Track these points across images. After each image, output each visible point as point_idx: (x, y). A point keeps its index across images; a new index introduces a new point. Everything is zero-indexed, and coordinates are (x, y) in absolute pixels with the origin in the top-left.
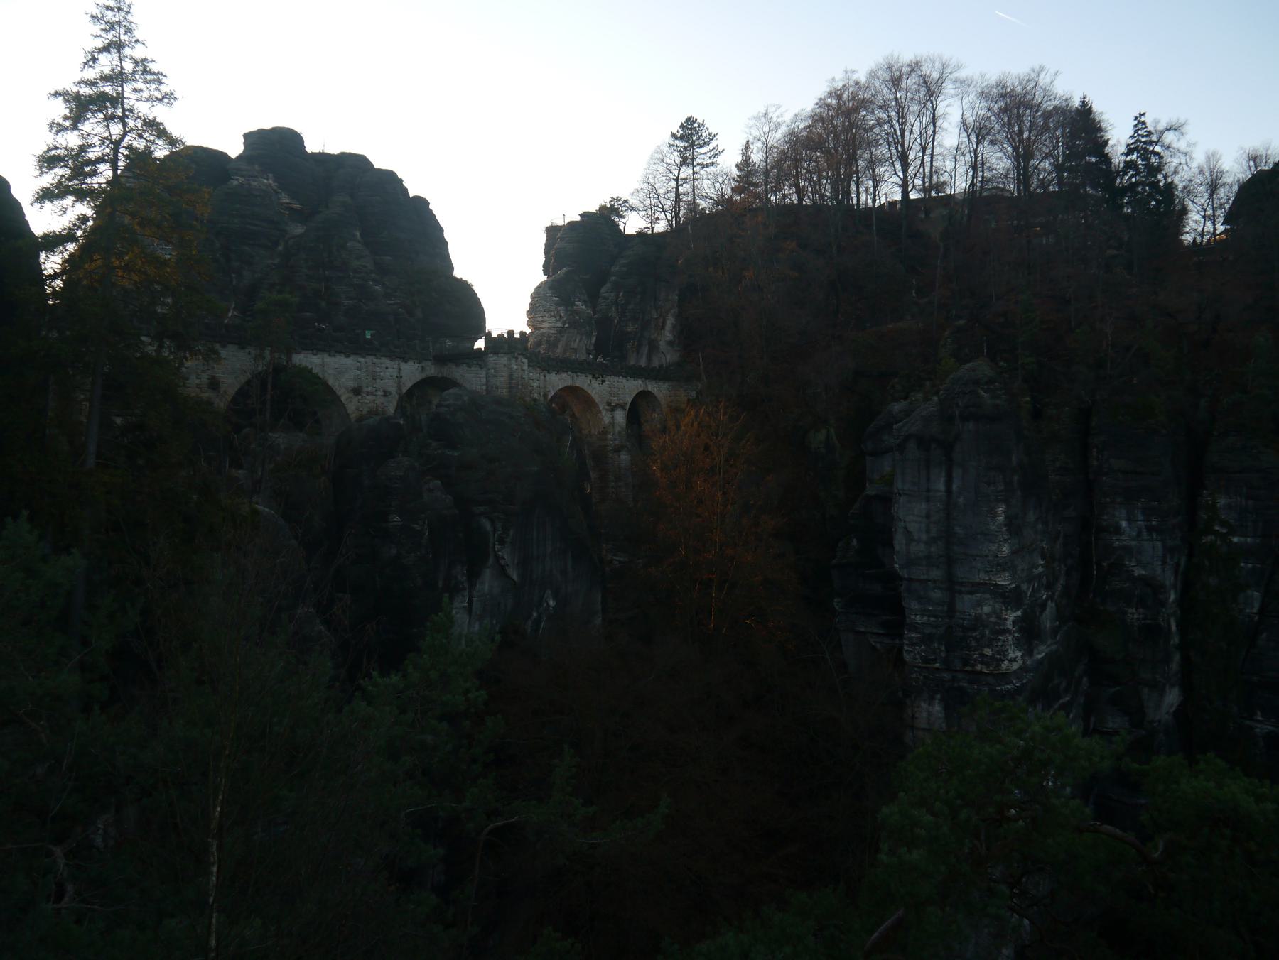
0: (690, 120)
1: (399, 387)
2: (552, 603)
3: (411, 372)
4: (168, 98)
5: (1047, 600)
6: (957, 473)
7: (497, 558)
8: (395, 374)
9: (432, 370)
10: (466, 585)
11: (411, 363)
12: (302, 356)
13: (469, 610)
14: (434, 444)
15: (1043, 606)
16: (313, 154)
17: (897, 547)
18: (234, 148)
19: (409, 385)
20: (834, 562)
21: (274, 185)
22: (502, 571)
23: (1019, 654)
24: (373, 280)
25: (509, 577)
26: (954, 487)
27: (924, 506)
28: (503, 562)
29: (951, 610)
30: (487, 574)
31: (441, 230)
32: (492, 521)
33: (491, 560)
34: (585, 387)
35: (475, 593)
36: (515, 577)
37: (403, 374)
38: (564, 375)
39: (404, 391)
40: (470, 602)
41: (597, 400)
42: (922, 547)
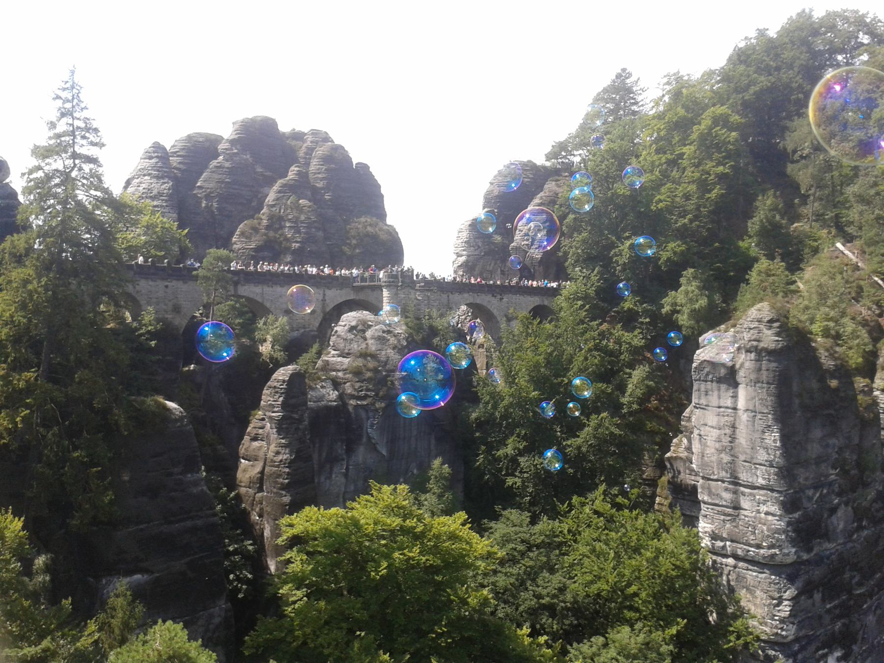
0: (623, 75)
1: (324, 307)
2: (415, 471)
3: (335, 296)
4: (101, 145)
5: (839, 504)
6: (742, 392)
7: (369, 438)
8: (321, 298)
9: (352, 296)
10: (345, 457)
11: (334, 290)
12: (246, 287)
13: (346, 475)
14: (333, 352)
15: (833, 510)
16: (284, 134)
17: (694, 450)
18: (226, 130)
19: (331, 306)
20: (668, 455)
21: (250, 160)
22: (373, 448)
23: (793, 550)
24: (315, 228)
25: (378, 452)
26: (741, 404)
27: (716, 419)
28: (373, 441)
29: (737, 507)
30: (361, 449)
31: (378, 187)
32: (367, 411)
33: (364, 440)
34: (485, 304)
35: (351, 463)
36: (384, 453)
37: (326, 298)
38: (466, 295)
39: (328, 310)
40: (347, 469)
41: (495, 312)
42: (713, 450)
